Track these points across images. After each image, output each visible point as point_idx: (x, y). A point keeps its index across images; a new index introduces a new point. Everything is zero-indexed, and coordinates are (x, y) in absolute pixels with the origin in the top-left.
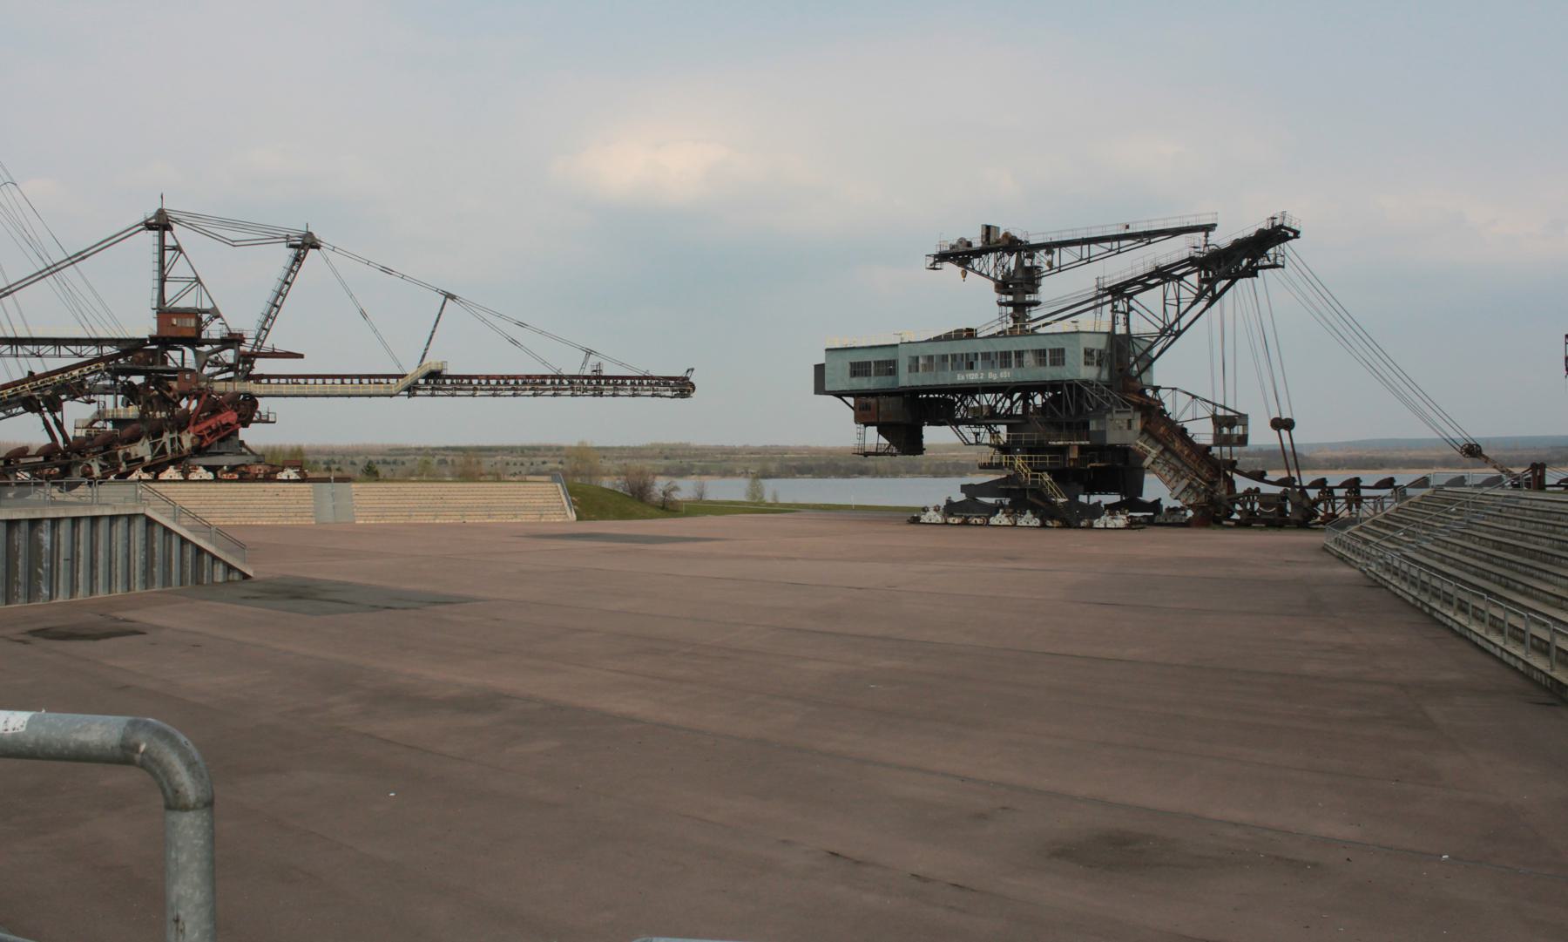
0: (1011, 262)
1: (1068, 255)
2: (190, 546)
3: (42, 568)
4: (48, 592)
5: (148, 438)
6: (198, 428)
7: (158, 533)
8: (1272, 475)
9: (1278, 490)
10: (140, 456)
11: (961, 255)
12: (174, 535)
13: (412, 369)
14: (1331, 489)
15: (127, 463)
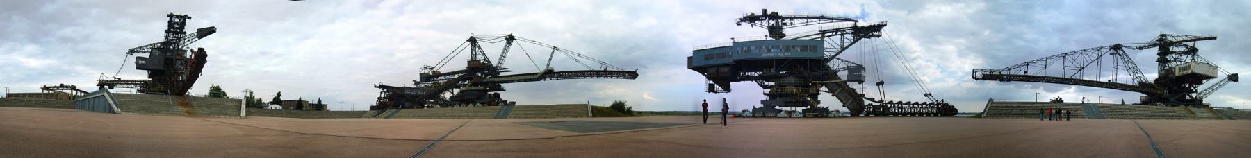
0: (773, 22)
1: (796, 21)
8: (877, 100)
9: (878, 104)
11: (752, 19)
13: (542, 69)
14: (894, 104)
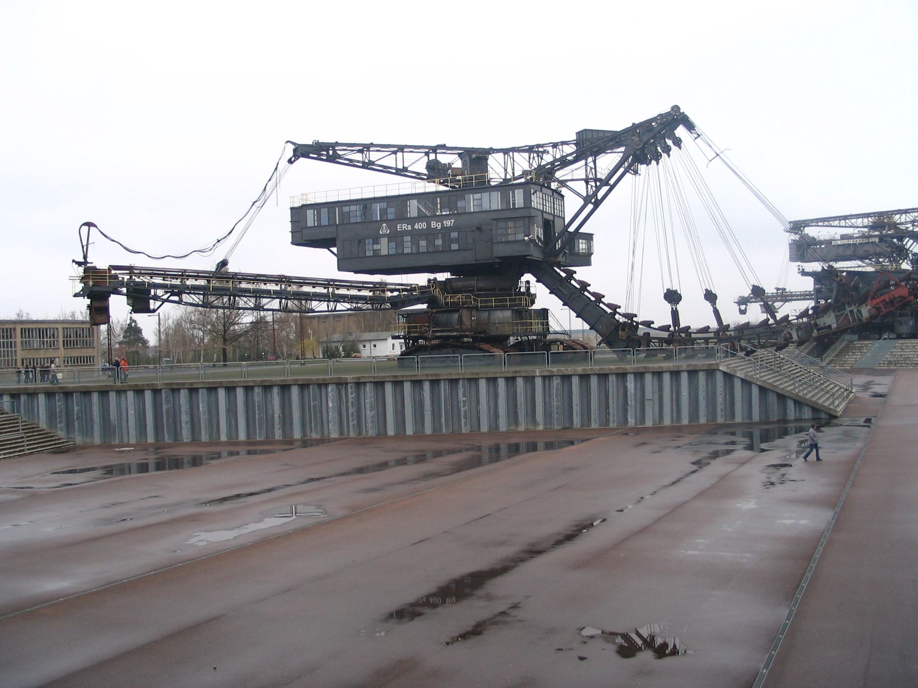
2: (770, 391)
3: (628, 405)
4: (633, 421)
5: (834, 311)
6: (875, 302)
7: (738, 384)
10: (827, 324)
12: (754, 387)
15: (817, 331)
